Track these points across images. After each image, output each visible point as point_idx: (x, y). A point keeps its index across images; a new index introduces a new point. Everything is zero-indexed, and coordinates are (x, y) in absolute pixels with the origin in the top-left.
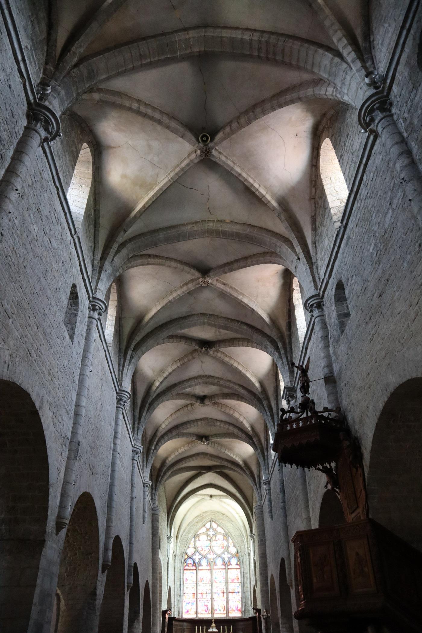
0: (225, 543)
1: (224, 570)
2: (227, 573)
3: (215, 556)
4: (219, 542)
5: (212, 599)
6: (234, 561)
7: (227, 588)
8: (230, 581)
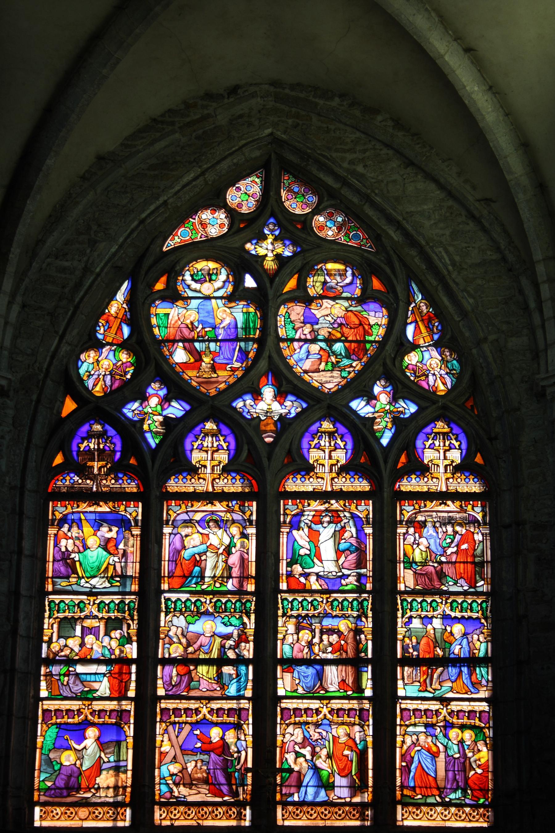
0: (377, 319)
1: (365, 509)
2: (385, 528)
3: (291, 407)
4: (329, 312)
5: (265, 701)
6: (441, 454)
7: (385, 632)
8: (407, 579)
